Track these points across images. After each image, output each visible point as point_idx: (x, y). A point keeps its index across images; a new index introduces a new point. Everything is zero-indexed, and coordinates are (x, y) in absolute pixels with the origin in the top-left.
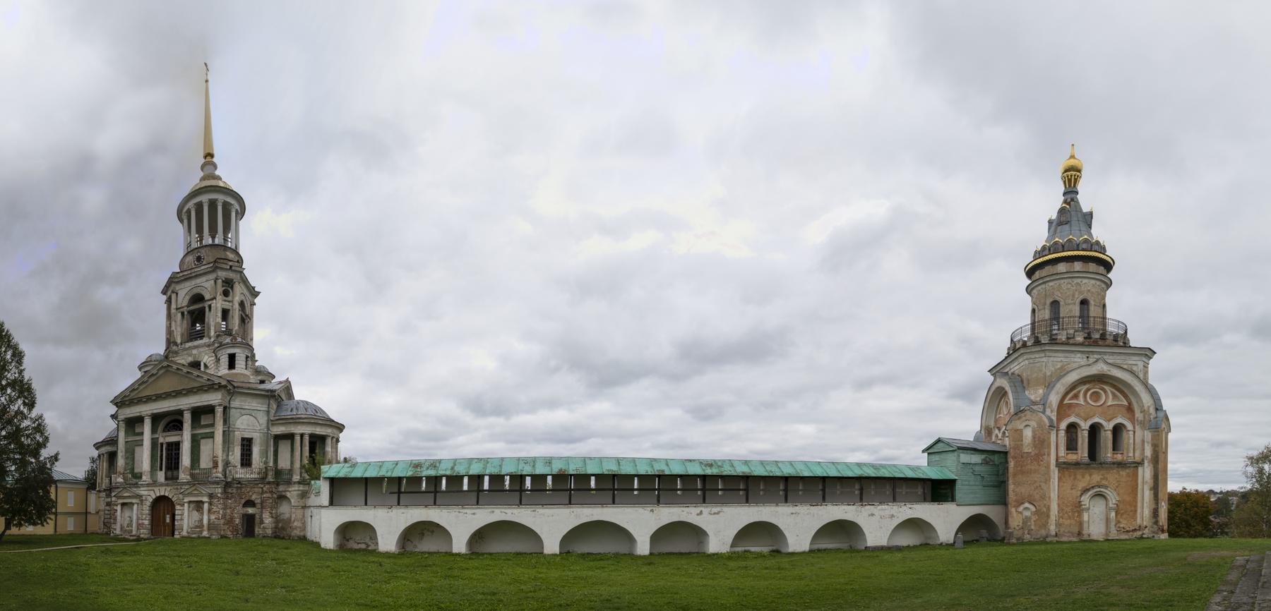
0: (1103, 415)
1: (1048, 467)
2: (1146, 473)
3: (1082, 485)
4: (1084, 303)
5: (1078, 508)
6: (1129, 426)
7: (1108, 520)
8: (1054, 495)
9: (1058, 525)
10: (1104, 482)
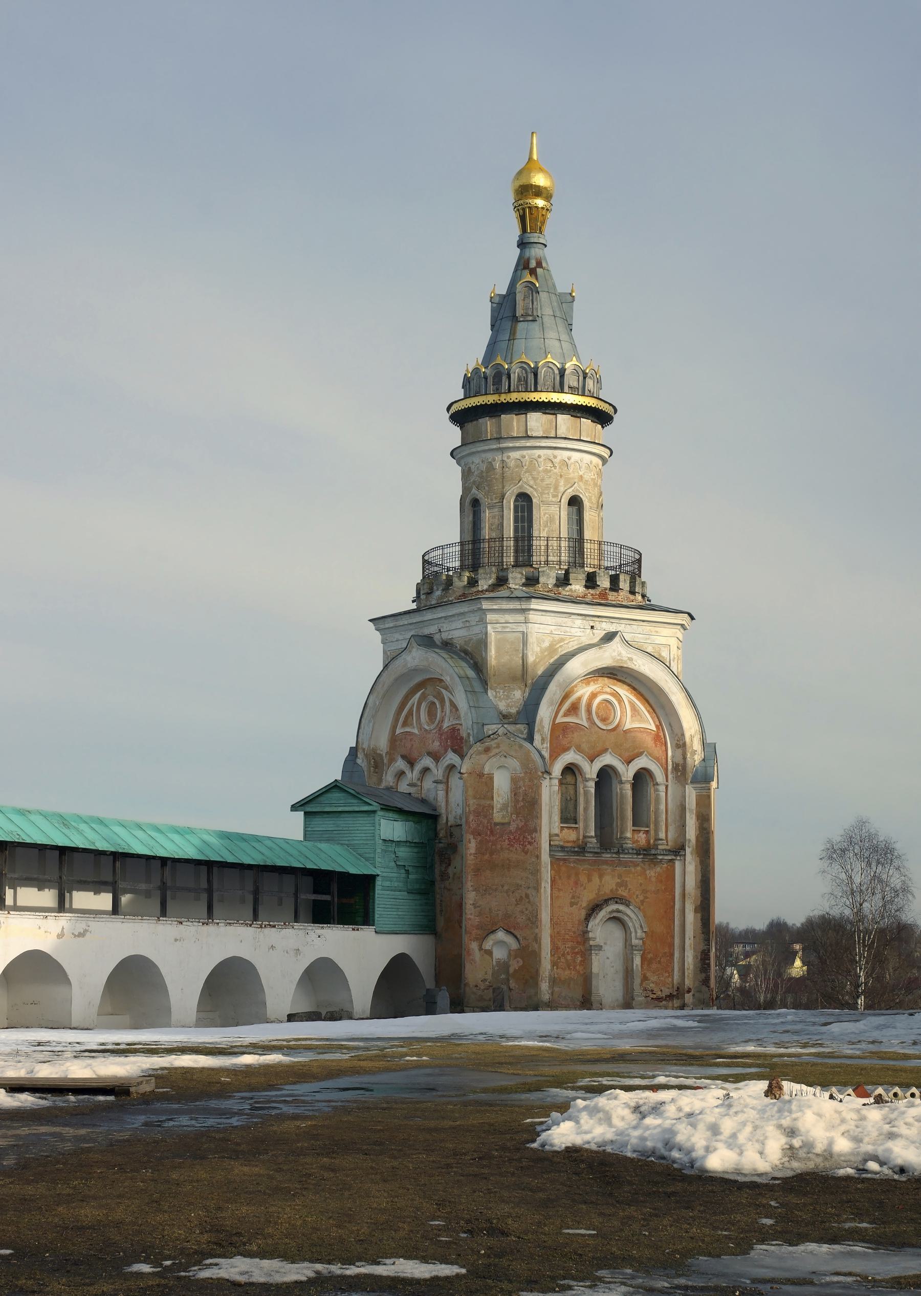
0: (618, 750)
1: (538, 857)
2: (687, 871)
3: (588, 896)
4: (575, 502)
5: (582, 946)
6: (659, 776)
7: (628, 973)
8: (545, 916)
9: (554, 981)
10: (622, 892)
